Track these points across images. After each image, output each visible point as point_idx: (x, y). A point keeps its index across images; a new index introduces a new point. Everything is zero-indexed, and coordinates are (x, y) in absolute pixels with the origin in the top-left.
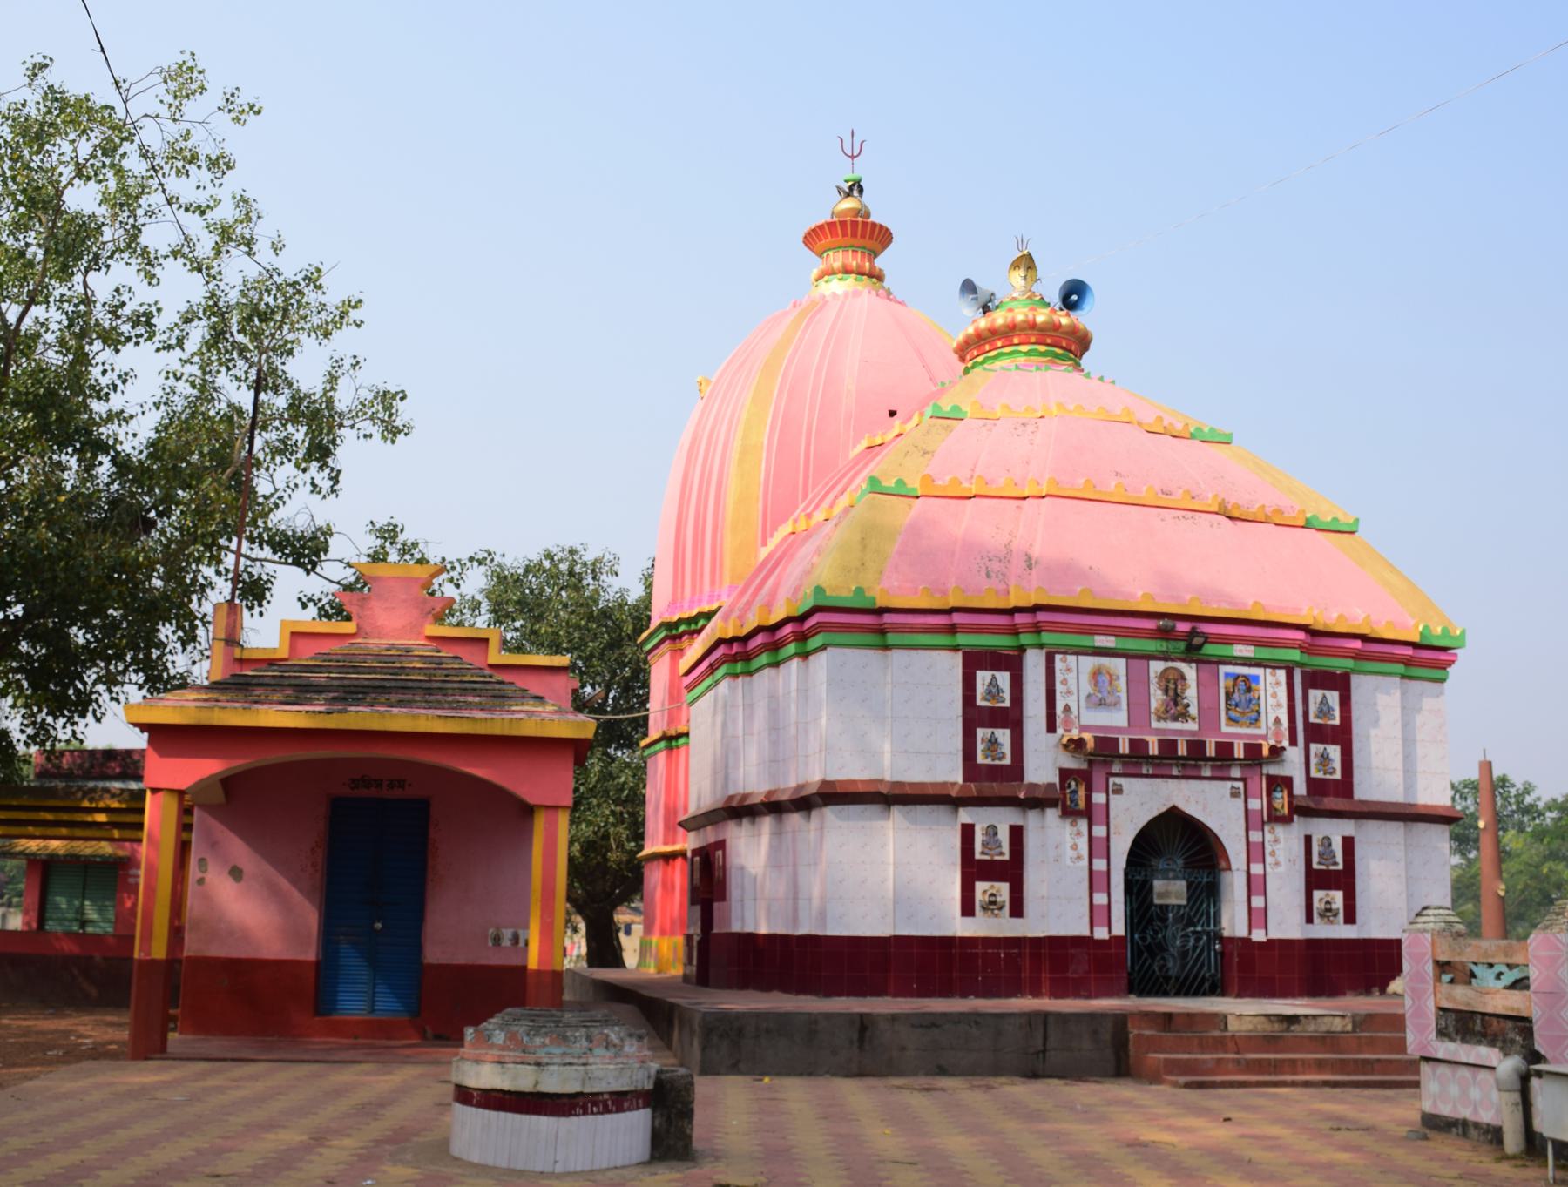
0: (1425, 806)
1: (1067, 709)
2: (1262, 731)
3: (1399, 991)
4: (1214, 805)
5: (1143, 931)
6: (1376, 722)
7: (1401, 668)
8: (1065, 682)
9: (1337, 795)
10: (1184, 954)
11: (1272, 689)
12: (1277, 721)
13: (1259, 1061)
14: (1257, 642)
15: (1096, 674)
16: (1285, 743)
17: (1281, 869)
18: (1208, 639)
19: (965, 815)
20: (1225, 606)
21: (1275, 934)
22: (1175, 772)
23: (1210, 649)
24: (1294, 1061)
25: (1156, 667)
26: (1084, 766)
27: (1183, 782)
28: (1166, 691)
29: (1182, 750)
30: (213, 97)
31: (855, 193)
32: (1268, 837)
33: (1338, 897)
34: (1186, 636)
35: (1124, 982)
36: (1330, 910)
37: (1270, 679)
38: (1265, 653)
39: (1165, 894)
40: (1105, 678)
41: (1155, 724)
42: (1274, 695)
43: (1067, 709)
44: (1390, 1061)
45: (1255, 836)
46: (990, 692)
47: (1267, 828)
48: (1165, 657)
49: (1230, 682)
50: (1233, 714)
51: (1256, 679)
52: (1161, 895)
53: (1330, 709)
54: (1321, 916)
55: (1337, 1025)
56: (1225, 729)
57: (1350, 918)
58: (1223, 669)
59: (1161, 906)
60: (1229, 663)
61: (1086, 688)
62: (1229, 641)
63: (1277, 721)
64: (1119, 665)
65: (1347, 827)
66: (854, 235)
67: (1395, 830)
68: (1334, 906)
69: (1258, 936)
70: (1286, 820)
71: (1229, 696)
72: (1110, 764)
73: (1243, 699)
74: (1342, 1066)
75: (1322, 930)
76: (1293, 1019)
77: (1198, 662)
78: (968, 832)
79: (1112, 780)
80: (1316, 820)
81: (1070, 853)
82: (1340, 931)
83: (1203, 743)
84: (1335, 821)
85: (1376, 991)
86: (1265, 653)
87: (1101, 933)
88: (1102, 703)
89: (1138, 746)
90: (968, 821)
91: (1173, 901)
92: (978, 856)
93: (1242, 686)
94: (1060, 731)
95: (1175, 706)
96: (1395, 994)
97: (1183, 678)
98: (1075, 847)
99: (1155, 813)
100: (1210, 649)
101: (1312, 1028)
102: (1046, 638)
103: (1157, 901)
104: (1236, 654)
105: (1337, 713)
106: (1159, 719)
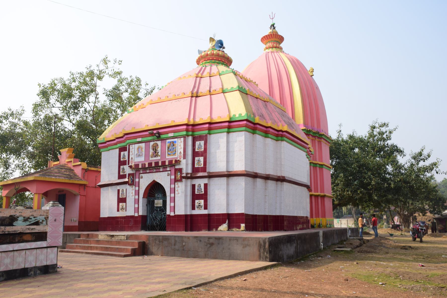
0: (235, 172)
1: (132, 158)
2: (176, 156)
3: (222, 230)
4: (163, 178)
5: (152, 214)
6: (219, 148)
7: (226, 130)
8: (132, 152)
9: (202, 172)
10: (161, 220)
11: (179, 143)
12: (180, 153)
13: (107, 248)
14: (174, 132)
15: (138, 148)
16: (182, 159)
17: (179, 195)
18: (160, 134)
19: (118, 187)
20: (165, 124)
21: (176, 214)
22: (155, 171)
23: (162, 136)
24: (91, 247)
25: (152, 143)
26: (134, 172)
27: (156, 173)
28: (153, 150)
29: (153, 165)
30: (112, 62)
31: (272, 28)
32: (176, 186)
33: (202, 202)
34: (157, 134)
35: (140, 227)
36: (200, 206)
37: (179, 141)
38: (176, 134)
39: (157, 204)
40: (140, 149)
41: (150, 159)
42: (180, 146)
43: (132, 158)
44: (112, 248)
45: (173, 186)
46: (123, 157)
47: (176, 183)
48: (153, 140)
49: (169, 144)
50: (169, 153)
51: (176, 142)
52: (157, 204)
53: (201, 146)
54: (197, 207)
55: (123, 238)
56: (167, 157)
57: (206, 208)
58: (167, 141)
59: (156, 207)
60: (169, 139)
61: (136, 152)
62: (167, 133)
63: (180, 153)
64: (143, 145)
65: (206, 181)
66: (268, 39)
67: (224, 180)
68: (201, 205)
69: (172, 214)
70: (180, 181)
71: (168, 148)
72: (139, 171)
73: (172, 148)
74: (102, 249)
75: (197, 212)
76: (113, 236)
77: (161, 140)
78: (119, 191)
79: (140, 175)
80: (197, 179)
81: (131, 195)
82: (203, 212)
83: (158, 162)
84: (202, 179)
85: (214, 230)
86: (176, 134)
87: (136, 215)
88: (139, 156)
89: (144, 165)
90: (119, 189)
91: (159, 205)
92: (120, 197)
93: (172, 144)
94: (130, 164)
95: (156, 153)
96: (220, 230)
97: (158, 145)
98: (132, 193)
99: (150, 182)
100: (162, 136)
101: (117, 239)
102: (128, 141)
103: (155, 206)
104: (169, 136)
105: (203, 147)
106: (152, 157)
